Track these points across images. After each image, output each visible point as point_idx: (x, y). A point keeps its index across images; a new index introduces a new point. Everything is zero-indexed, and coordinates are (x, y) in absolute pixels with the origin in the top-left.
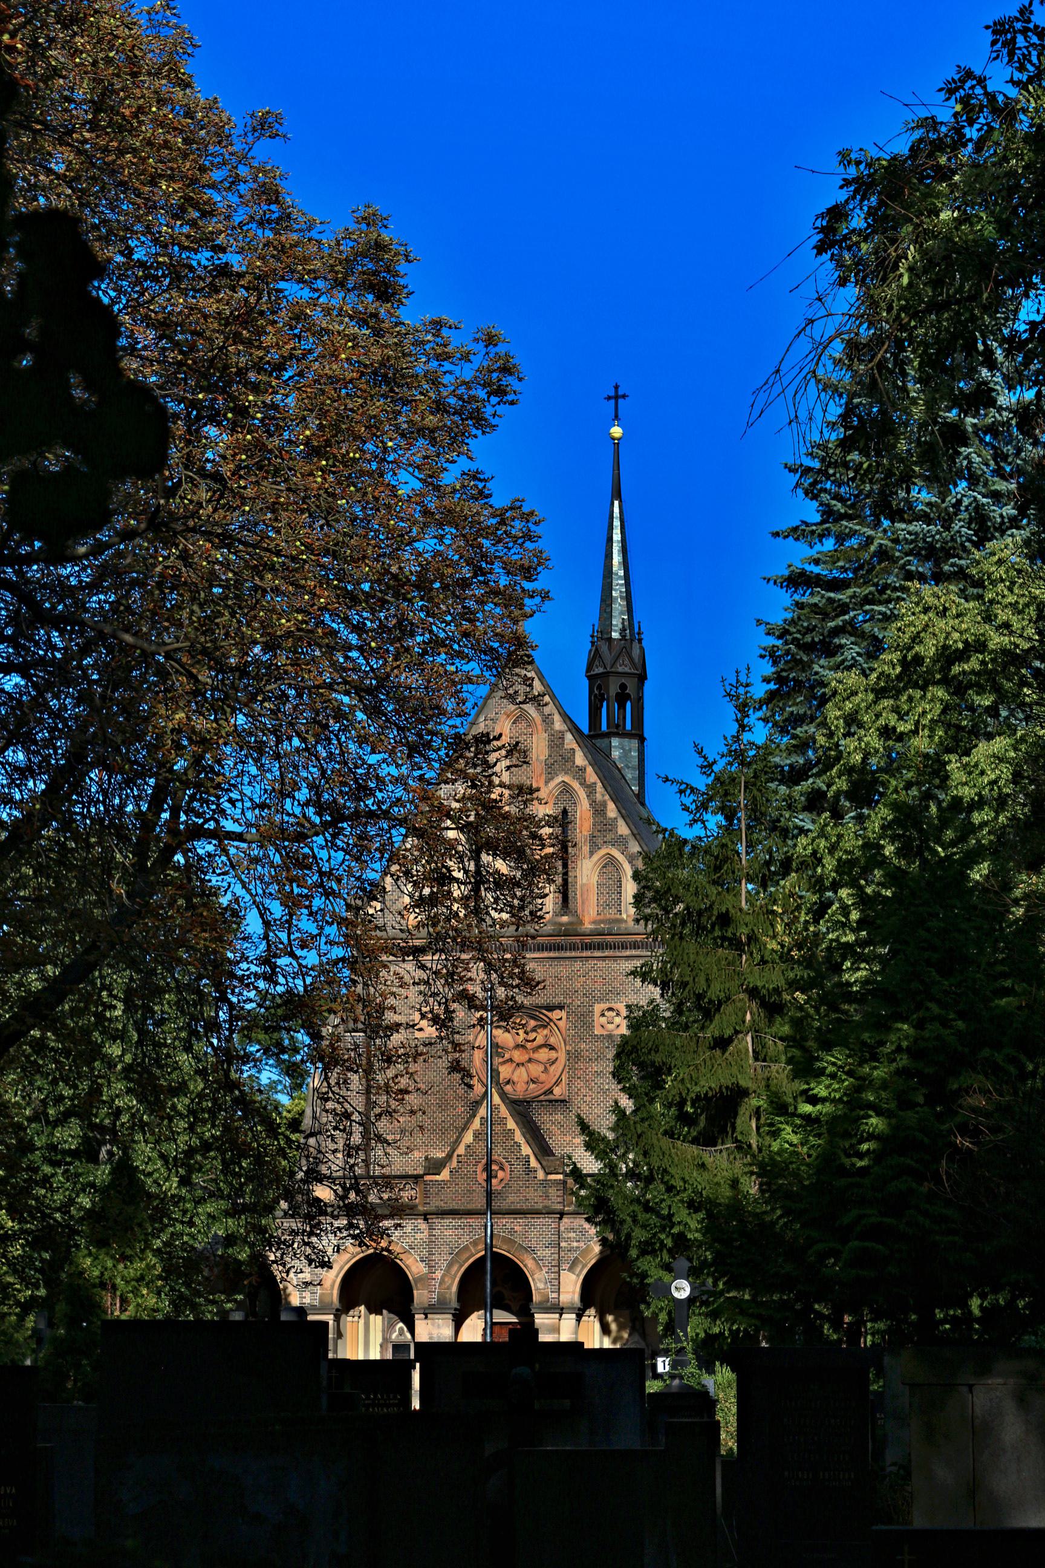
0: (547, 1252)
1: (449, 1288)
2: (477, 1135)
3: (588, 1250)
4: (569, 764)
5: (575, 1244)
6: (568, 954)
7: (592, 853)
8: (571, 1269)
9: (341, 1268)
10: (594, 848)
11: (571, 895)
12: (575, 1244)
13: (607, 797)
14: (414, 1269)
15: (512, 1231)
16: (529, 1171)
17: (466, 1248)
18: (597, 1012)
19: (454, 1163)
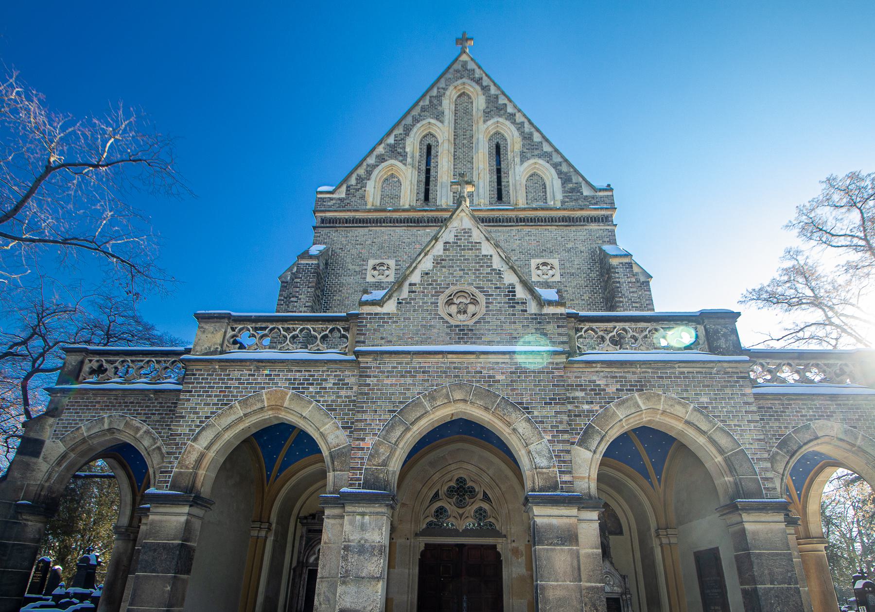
0: (549, 411)
1: (385, 464)
2: (438, 262)
3: (606, 416)
5: (586, 407)
7: (522, 162)
8: (582, 443)
9: (218, 436)
10: (524, 158)
11: (504, 193)
12: (586, 407)
13: (533, 130)
14: (331, 439)
17: (417, 404)
18: (534, 262)
19: (405, 293)
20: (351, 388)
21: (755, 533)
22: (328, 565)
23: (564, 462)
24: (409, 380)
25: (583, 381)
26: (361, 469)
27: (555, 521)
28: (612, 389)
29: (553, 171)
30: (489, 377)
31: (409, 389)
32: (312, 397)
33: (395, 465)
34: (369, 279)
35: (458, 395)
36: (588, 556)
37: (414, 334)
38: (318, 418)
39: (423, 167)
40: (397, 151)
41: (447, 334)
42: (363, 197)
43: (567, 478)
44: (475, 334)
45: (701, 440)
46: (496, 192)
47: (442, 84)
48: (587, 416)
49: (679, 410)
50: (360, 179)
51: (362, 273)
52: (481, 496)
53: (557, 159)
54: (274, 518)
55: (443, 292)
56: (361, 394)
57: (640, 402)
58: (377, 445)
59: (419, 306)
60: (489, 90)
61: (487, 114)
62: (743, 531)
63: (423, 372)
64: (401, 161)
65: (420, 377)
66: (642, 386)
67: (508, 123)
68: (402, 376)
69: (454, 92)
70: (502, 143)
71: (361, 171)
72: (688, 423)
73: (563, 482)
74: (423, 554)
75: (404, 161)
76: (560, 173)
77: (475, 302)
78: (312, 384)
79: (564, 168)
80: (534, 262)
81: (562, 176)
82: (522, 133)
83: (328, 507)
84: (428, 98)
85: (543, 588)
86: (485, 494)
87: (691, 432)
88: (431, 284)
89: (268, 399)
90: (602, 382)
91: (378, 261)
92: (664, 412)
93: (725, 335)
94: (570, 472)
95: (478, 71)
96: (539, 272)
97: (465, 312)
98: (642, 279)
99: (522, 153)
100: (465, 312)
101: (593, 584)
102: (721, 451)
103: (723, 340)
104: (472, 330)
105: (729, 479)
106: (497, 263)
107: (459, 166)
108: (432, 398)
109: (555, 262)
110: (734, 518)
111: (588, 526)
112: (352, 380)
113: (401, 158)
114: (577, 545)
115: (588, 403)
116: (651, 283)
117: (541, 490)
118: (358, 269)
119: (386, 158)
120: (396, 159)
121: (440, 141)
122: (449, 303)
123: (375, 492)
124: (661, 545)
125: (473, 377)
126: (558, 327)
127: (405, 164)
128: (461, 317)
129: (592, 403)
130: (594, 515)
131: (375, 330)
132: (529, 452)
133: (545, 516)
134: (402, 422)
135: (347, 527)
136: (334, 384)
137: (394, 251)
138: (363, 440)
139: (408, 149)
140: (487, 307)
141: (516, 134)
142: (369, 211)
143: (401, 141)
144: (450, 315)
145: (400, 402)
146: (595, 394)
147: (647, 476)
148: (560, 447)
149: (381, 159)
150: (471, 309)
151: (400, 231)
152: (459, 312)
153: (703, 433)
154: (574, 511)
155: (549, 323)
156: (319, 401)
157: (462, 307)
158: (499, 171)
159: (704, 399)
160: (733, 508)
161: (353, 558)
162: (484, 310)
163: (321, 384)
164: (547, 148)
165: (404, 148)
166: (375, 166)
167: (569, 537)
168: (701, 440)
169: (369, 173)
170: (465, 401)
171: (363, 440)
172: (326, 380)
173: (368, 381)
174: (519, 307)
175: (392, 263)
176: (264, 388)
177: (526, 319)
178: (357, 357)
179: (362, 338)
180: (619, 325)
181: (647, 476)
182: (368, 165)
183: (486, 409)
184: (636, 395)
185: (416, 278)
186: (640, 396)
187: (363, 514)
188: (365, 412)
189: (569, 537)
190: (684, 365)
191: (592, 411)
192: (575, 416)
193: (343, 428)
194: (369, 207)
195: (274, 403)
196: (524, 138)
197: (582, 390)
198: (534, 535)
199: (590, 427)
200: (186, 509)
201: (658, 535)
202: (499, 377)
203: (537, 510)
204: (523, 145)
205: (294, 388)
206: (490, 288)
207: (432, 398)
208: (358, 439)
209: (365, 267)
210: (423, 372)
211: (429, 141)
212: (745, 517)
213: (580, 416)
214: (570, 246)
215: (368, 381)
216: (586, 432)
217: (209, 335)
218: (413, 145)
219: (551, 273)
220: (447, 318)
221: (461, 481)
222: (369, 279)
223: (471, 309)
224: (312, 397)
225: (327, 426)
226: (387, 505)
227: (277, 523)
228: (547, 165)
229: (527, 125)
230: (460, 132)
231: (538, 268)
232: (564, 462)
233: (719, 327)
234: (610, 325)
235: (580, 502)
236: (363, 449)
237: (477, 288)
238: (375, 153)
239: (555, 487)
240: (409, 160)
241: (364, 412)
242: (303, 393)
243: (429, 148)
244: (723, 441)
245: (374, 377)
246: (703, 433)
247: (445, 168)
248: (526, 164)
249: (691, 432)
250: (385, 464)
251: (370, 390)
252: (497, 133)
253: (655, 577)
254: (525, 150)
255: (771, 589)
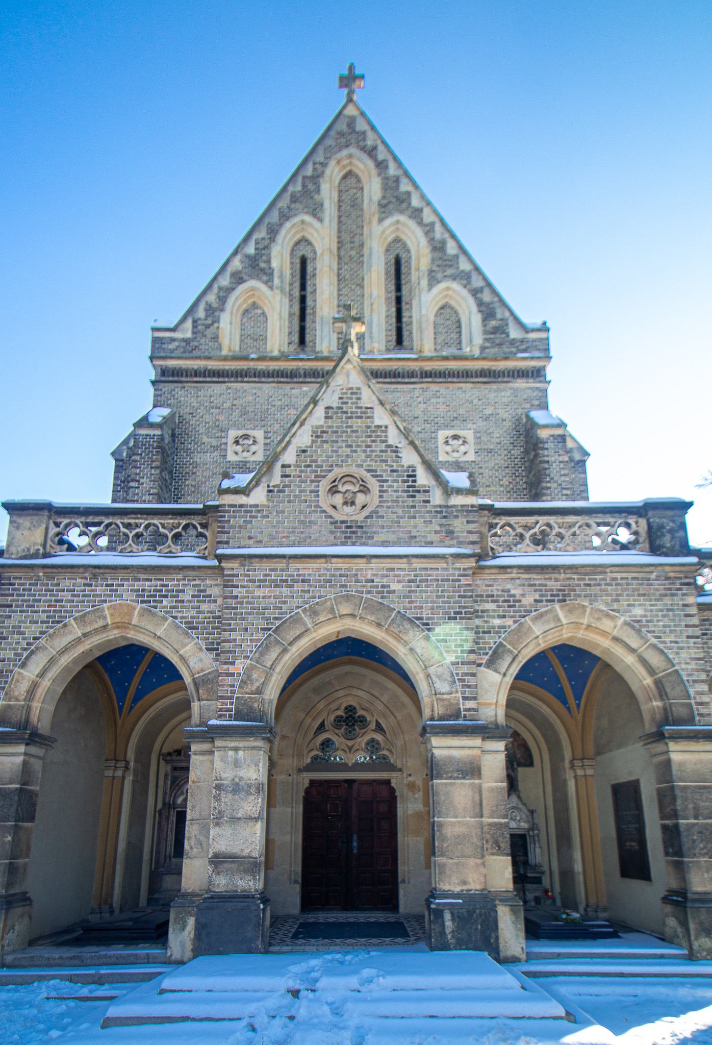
1: (259, 691)
3: (520, 631)
4: (404, 205)
5: (497, 622)
6: (406, 380)
7: (430, 286)
8: (491, 663)
10: (433, 281)
12: (497, 622)
14: (192, 662)
15: (385, 591)
16: (413, 490)
20: (215, 601)
21: (682, 764)
22: (197, 806)
23: (469, 686)
24: (285, 591)
25: (495, 590)
26: (231, 698)
27: (455, 753)
28: (528, 600)
29: (471, 301)
30: (383, 586)
31: (285, 603)
32: (167, 612)
33: (272, 693)
34: (231, 457)
35: (345, 609)
36: (492, 790)
37: (289, 533)
38: (175, 637)
39: (297, 293)
40: (257, 266)
41: (332, 532)
42: (215, 338)
43: (470, 704)
44: (365, 533)
45: (630, 659)
46: (394, 332)
47: (319, 157)
48: (497, 633)
49: (606, 625)
50: (210, 310)
51: (221, 449)
52: (373, 726)
53: (477, 282)
54: (131, 755)
55: (324, 477)
56: (227, 608)
57: (561, 615)
58: (249, 670)
59: (295, 496)
60: (387, 167)
61: (384, 209)
62: (668, 763)
63: (303, 581)
64: (266, 283)
65: (298, 587)
66: (564, 595)
67: (412, 224)
68: (276, 586)
69: (337, 170)
70: (403, 256)
71: (211, 298)
72: (616, 639)
73: (465, 710)
74: (307, 791)
75: (269, 283)
76: (480, 303)
77: (365, 490)
78: (166, 596)
79: (487, 297)
80: (442, 434)
81: (483, 309)
82: (432, 240)
83: (195, 742)
84: (300, 179)
85: (441, 825)
86: (378, 724)
87: (619, 651)
88: (309, 466)
89: (112, 615)
90: (517, 592)
91: (241, 433)
92: (589, 627)
93: (671, 531)
94: (475, 699)
95: (370, 134)
96: (448, 448)
97: (353, 503)
98: (577, 456)
99: (431, 272)
100: (353, 503)
101: (496, 820)
102: (651, 671)
103: (668, 537)
104: (361, 527)
105: (657, 704)
106: (393, 437)
107: (344, 292)
108: (314, 612)
109: (469, 435)
110: (659, 747)
111: (493, 757)
112: (215, 591)
113: (265, 278)
114: (480, 777)
115: (499, 617)
116: (587, 464)
117: (441, 718)
118: (215, 442)
119: (245, 277)
120: (259, 279)
121: (319, 251)
122: (333, 491)
123: (248, 724)
124: (576, 777)
125: (363, 586)
126: (468, 522)
127: (271, 288)
128: (348, 509)
129: (504, 617)
130: (501, 746)
131: (240, 527)
132: (428, 676)
133: (444, 748)
134: (277, 642)
135: (218, 764)
136: (193, 596)
137: (261, 418)
138: (233, 663)
139: (275, 264)
140: (381, 497)
141: (423, 241)
142: (225, 359)
143: (264, 249)
144: (335, 507)
145: (276, 619)
146: (509, 606)
147: (564, 701)
148: (465, 669)
149: (238, 279)
150: (361, 499)
151: (268, 389)
152: (345, 503)
153: (633, 651)
154: (477, 742)
155: (456, 517)
156: (176, 618)
157: (349, 496)
158: (399, 300)
159: (638, 612)
160: (659, 736)
161: (226, 798)
162: (376, 501)
163: (177, 596)
164: (464, 265)
165: (269, 261)
166: (230, 290)
167: (472, 770)
168: (630, 659)
169: (223, 300)
170: (353, 616)
171: (233, 663)
172: (183, 591)
173: (235, 592)
174: (420, 497)
175: (259, 434)
176: (105, 601)
177: (428, 512)
178: (220, 562)
179: (225, 538)
180: (543, 519)
181: (564, 701)
182: (220, 289)
183: (379, 625)
184: (557, 606)
185: (289, 457)
186: (561, 607)
187: (236, 749)
188: (234, 630)
189: (472, 770)
190: (616, 569)
191: (504, 627)
192: (484, 632)
193: (208, 649)
194: (225, 352)
195: (118, 620)
196: (434, 249)
197: (493, 601)
198: (433, 769)
199: (501, 644)
200: (22, 748)
201: (572, 767)
202: (394, 586)
203: (435, 741)
204: (433, 260)
205: (142, 602)
206: (385, 471)
207: (314, 612)
208: (226, 663)
209: (224, 441)
210: (303, 581)
211: (304, 251)
212: (672, 746)
213: (489, 632)
214: (488, 411)
215: (235, 592)
216: (495, 652)
217: (26, 533)
218: (281, 259)
219: (463, 449)
220: (331, 511)
221: (350, 709)
222: (231, 457)
223: (361, 499)
224: (167, 612)
225: (188, 648)
226: (264, 739)
227: (136, 761)
228: (465, 293)
229: (438, 228)
230: (346, 237)
231: (447, 443)
232: (469, 686)
233: (665, 520)
234: (531, 520)
235: (486, 731)
236: (232, 675)
237: (369, 471)
238: (230, 269)
239: (457, 715)
240: (276, 281)
241: (231, 630)
242: (156, 607)
243: (304, 262)
244: (655, 660)
245: (243, 587)
246: (633, 651)
247: (326, 295)
248: (435, 290)
249: (619, 651)
250: (259, 691)
251: (238, 603)
252: (397, 240)
253: (566, 810)
254: (435, 268)
255: (694, 825)
